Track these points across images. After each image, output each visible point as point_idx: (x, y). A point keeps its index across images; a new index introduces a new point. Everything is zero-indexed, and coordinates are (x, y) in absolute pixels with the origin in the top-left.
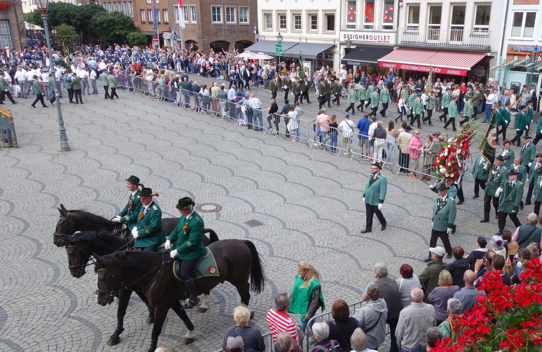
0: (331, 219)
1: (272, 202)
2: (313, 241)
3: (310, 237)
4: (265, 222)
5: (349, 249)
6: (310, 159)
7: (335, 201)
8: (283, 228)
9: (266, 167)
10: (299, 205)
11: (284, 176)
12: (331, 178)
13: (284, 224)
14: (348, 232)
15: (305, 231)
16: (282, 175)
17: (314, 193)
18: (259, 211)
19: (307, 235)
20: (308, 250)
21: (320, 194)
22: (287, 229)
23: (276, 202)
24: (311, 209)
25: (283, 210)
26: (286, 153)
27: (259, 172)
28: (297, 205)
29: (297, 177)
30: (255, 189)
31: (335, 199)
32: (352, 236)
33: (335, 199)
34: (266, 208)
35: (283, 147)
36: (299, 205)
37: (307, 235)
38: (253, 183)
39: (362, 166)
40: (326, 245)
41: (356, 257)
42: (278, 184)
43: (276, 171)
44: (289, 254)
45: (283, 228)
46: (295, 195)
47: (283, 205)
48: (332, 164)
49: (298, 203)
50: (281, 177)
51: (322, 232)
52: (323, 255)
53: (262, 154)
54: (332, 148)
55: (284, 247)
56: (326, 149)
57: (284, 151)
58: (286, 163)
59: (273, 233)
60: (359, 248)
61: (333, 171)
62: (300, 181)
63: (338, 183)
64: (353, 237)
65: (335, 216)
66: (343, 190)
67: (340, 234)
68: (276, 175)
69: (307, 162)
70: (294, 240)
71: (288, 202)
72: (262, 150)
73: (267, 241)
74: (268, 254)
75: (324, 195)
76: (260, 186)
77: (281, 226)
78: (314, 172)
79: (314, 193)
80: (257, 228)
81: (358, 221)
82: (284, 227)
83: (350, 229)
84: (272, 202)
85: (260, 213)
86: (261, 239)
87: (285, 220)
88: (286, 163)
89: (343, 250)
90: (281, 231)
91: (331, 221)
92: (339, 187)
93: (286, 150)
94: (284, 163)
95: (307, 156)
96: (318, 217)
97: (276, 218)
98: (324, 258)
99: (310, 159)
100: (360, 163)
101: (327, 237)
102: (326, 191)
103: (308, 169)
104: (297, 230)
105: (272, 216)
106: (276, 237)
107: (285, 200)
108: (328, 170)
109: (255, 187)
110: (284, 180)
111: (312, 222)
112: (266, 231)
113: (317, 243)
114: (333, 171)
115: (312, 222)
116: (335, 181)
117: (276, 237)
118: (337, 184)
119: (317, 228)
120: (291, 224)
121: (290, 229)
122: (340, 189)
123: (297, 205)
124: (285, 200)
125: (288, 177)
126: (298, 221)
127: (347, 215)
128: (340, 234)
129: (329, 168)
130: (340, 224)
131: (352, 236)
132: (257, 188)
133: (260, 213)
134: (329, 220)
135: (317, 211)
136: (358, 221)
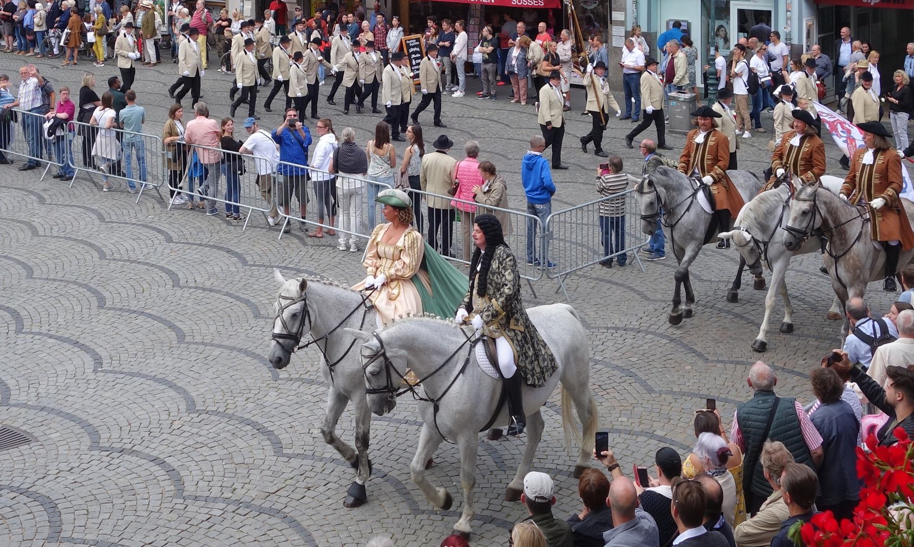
0: (230, 412)
1: (59, 369)
2: (179, 482)
3: (171, 471)
4: (37, 433)
5: (284, 500)
6: (169, 240)
7: (241, 356)
8: (91, 448)
9: (44, 269)
10: (139, 375)
11: (95, 292)
12: (226, 289)
13: (94, 433)
14: (278, 447)
15: (155, 454)
16: (90, 289)
17: (181, 337)
18: (23, 398)
19: (162, 463)
20: (166, 512)
21: (198, 339)
22: (102, 449)
23: (71, 368)
24: (172, 386)
25: (90, 392)
26: (103, 226)
27: (25, 283)
28: (132, 375)
29: (131, 293)
30: (12, 334)
31: (240, 350)
32: (290, 457)
33: (240, 350)
34: (42, 391)
35: (93, 211)
36: (139, 375)
37: (162, 463)
38: (8, 316)
39: (312, 251)
40: (215, 492)
41: (305, 524)
42: (77, 317)
43: (73, 278)
44: (107, 529)
45: (91, 448)
46: (127, 345)
47: (92, 376)
48: (229, 251)
49: (135, 369)
50: (88, 294)
51: (205, 451)
52: (207, 524)
53: (35, 232)
54: (228, 207)
55: (94, 508)
56: (213, 210)
57: (97, 222)
58: (102, 255)
59: (63, 466)
60: (310, 494)
61: (233, 269)
62: (142, 304)
63: (247, 302)
64: (295, 463)
65: (240, 401)
66: (262, 322)
67: (259, 454)
68: (73, 289)
69: (160, 249)
70: (122, 482)
71: (106, 367)
72: (36, 221)
73: (42, 491)
74: (46, 532)
75: (208, 339)
76: (27, 323)
77: (87, 441)
78: (180, 275)
79: (181, 337)
80: (14, 452)
81: (305, 412)
82: (95, 445)
83: (285, 438)
84: (59, 369)
85: (25, 406)
86: (25, 486)
87: (96, 422)
88: (102, 255)
89: (267, 505)
90: (86, 458)
91: (231, 417)
92: (250, 314)
93: (101, 218)
94: (96, 254)
95: (159, 231)
96: (191, 407)
97: (71, 417)
98: (212, 533)
99: (169, 240)
100: (305, 244)
101: (218, 468)
102: (213, 329)
103: (162, 269)
104: (132, 452)
105: (59, 413)
106: (71, 478)
107: (98, 361)
108: (217, 269)
109: (13, 328)
110: (95, 302)
111: (177, 425)
112: (41, 461)
113: (190, 488)
114: (233, 269)
115: (177, 425)
116: (238, 298)
117: (71, 478)
118: (243, 305)
119: (191, 442)
120: (115, 434)
121: (110, 450)
122: (252, 321)
123: (132, 375)
124: (98, 361)
125: (106, 294)
126: (135, 425)
127: (273, 394)
128: (259, 454)
129: (221, 263)
130: (254, 424)
131: (290, 457)
132: (19, 331)
133: (25, 406)
134: (224, 414)
135: (189, 389)
136: (305, 412)
